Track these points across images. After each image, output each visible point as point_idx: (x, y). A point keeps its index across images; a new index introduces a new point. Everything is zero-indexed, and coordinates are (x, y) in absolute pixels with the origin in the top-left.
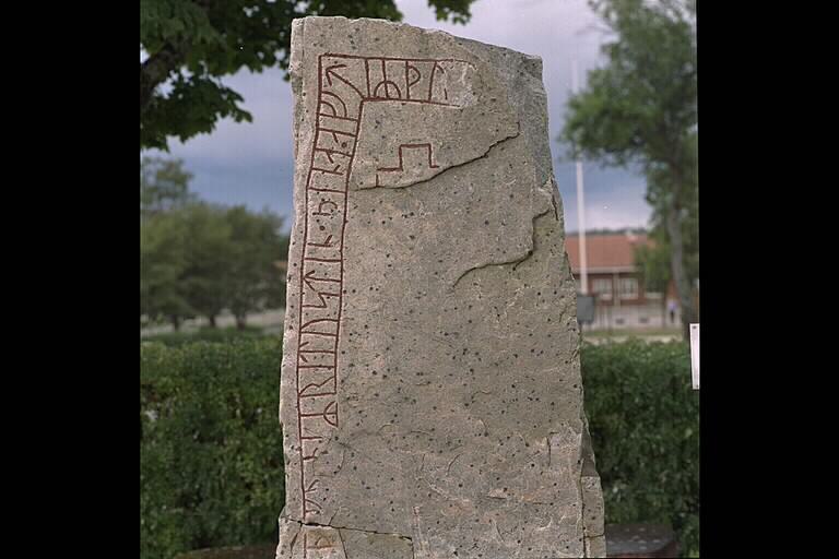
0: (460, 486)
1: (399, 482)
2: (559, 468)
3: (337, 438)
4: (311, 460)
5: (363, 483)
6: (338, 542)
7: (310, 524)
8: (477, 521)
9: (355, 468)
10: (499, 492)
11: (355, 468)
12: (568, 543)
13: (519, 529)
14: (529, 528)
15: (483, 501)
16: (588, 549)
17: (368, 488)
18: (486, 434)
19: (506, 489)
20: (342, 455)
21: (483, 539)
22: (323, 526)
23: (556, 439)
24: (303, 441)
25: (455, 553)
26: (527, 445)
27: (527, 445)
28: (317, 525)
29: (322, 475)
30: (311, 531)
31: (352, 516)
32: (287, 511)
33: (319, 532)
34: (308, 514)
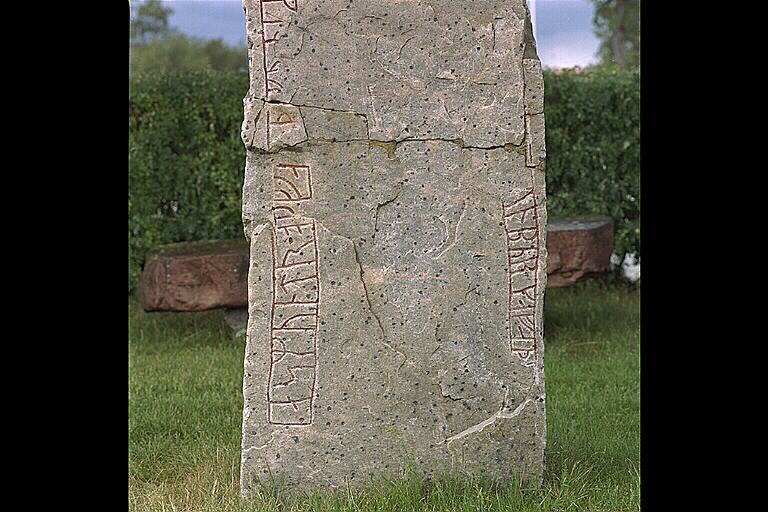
0: (411, 67)
1: (354, 63)
2: (503, 50)
3: (296, 22)
4: (273, 42)
5: (321, 65)
6: (299, 118)
7: (272, 102)
8: (427, 100)
9: (313, 51)
10: (447, 73)
11: (313, 51)
12: (510, 121)
13: (466, 107)
14: (475, 105)
15: (434, 82)
16: (528, 126)
17: (326, 69)
18: (436, 19)
19: (453, 71)
20: (301, 38)
21: (432, 117)
22: (284, 103)
23: (500, 24)
24: (265, 24)
25: (406, 129)
26: (474, 30)
27: (474, 30)
28: (279, 102)
29: (282, 56)
30: (273, 108)
31: (311, 95)
32: (251, 91)
33: (280, 109)
34: (270, 93)
